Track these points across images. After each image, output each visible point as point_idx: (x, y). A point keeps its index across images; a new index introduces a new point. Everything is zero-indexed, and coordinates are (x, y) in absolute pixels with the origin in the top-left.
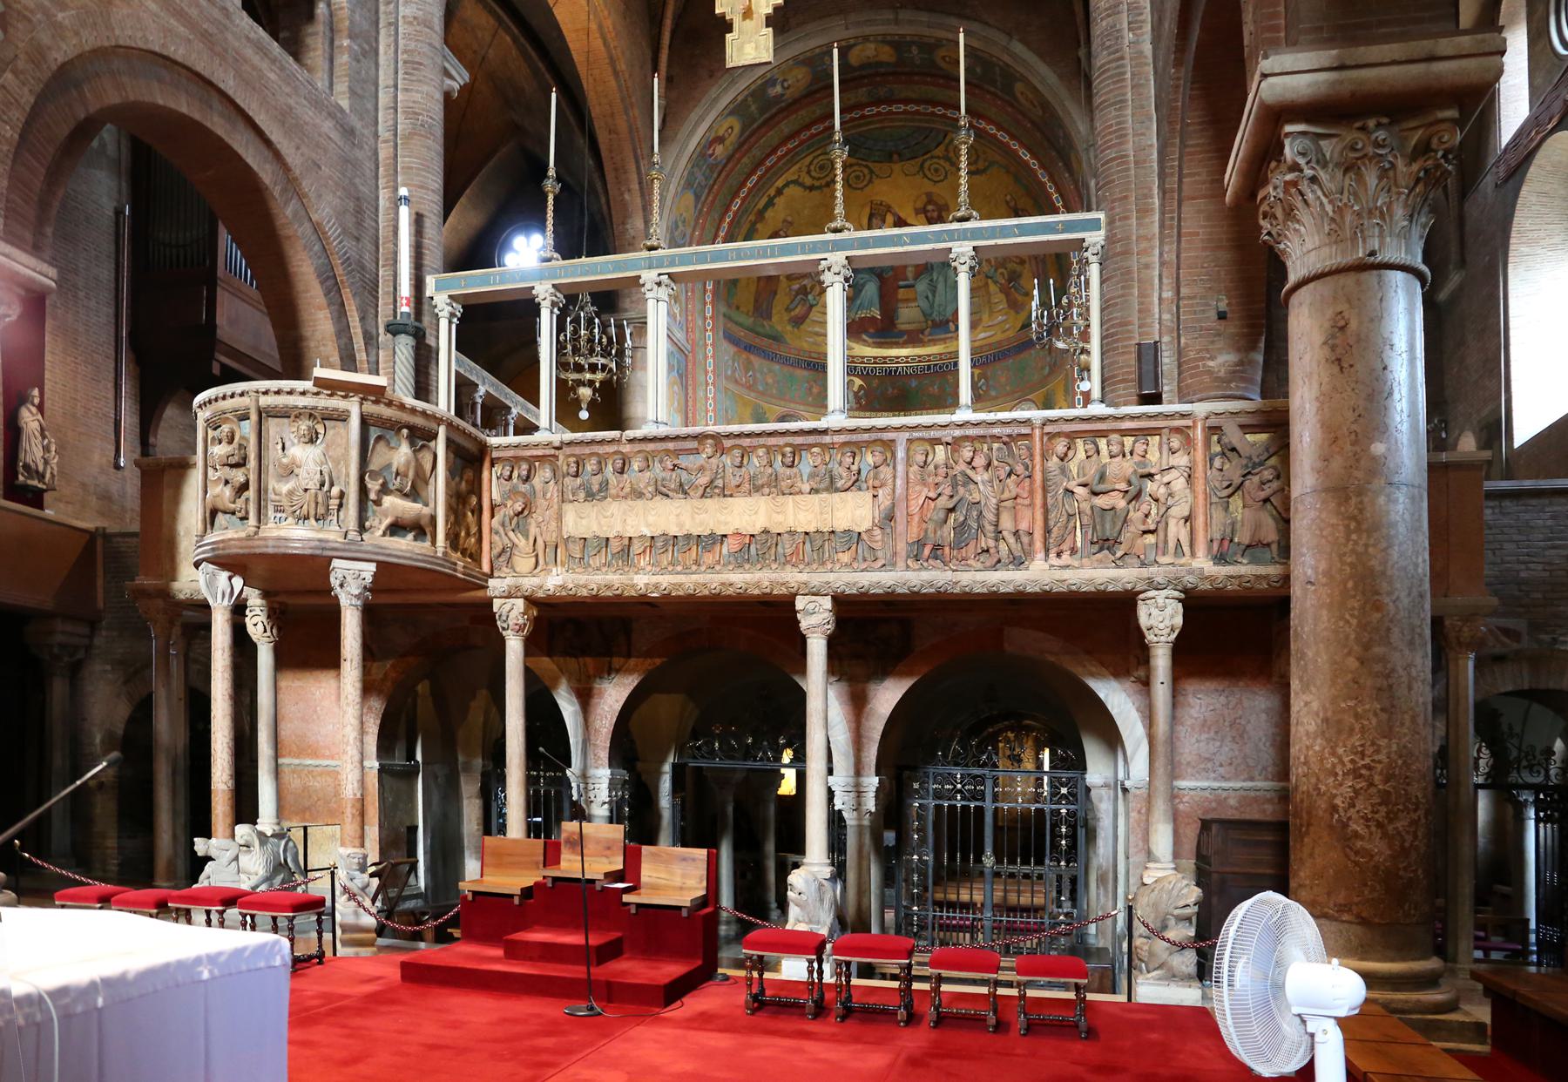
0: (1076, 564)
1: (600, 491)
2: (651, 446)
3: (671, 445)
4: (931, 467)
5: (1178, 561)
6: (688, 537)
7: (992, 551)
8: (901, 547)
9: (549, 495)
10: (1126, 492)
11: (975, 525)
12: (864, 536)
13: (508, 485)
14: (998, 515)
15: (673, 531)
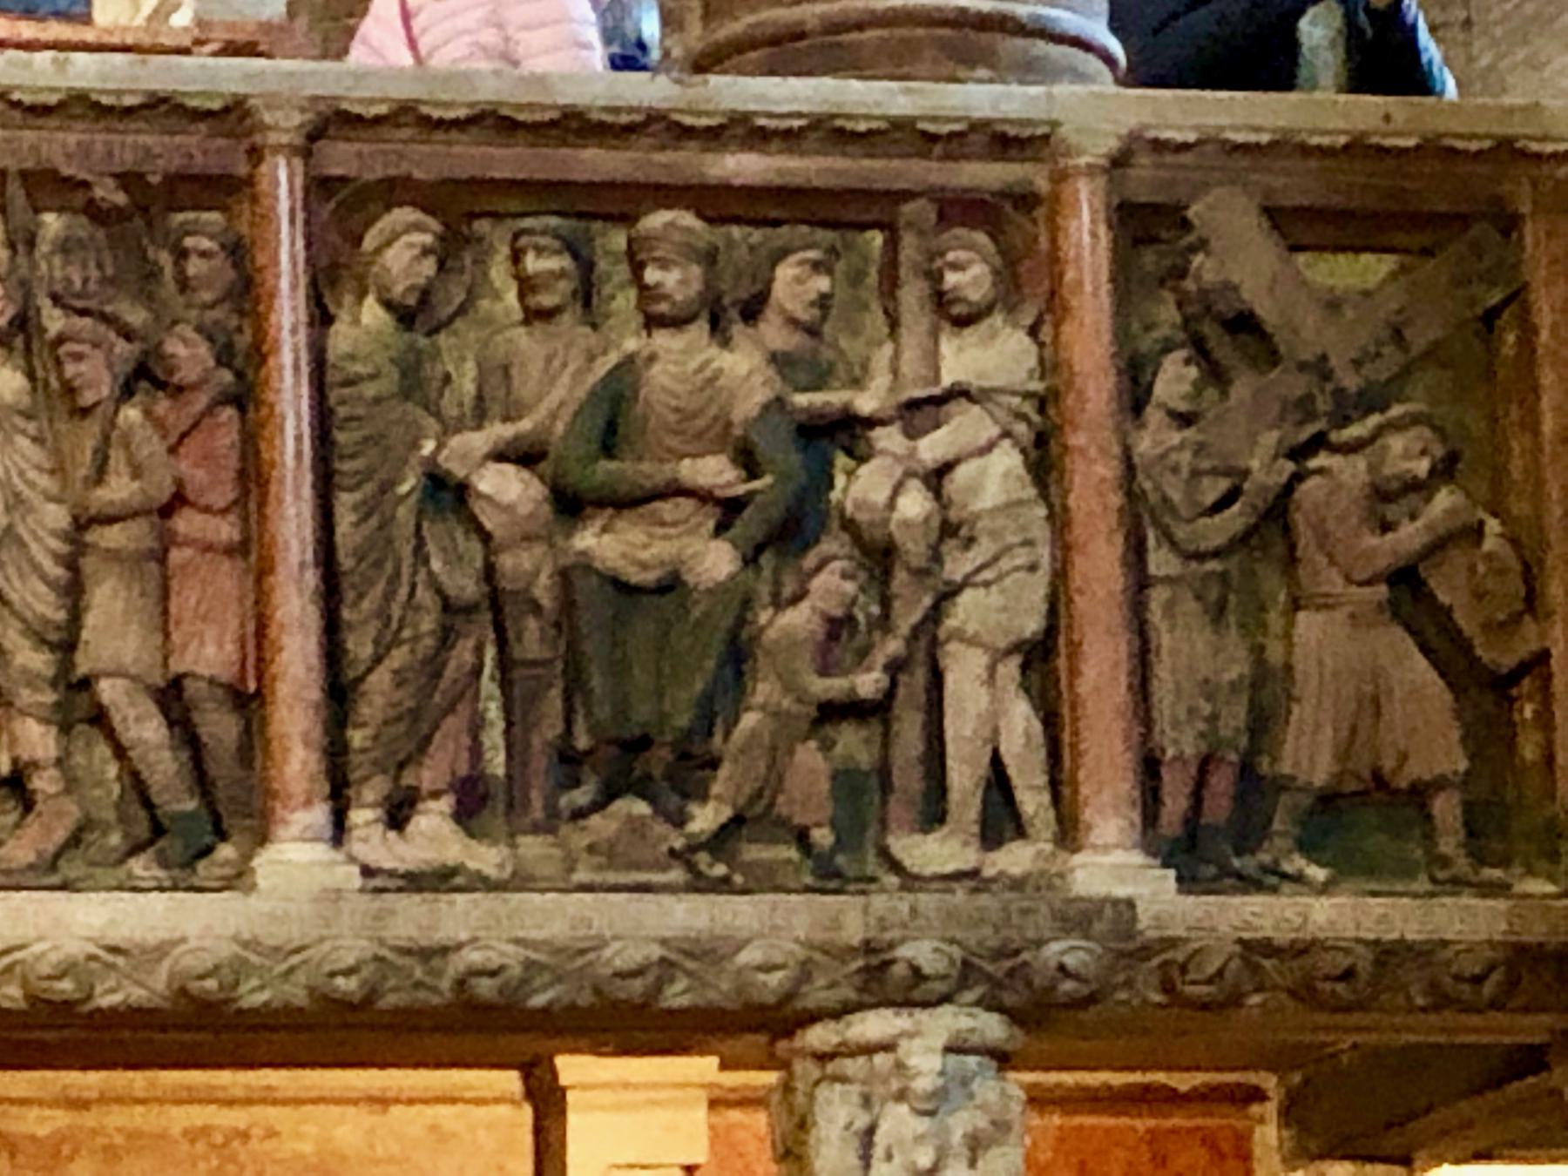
7: (44, 783)
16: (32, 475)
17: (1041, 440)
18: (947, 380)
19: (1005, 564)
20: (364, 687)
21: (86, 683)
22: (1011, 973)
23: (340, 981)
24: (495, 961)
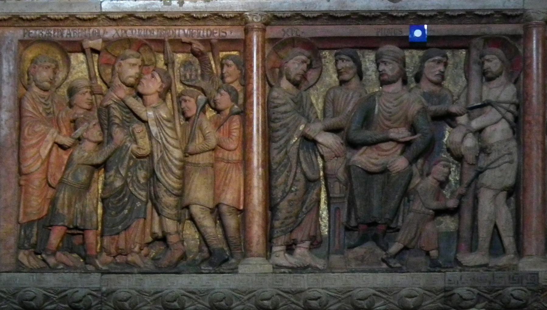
0: (320, 263)
4: (63, 91)
5: (494, 262)
7: (172, 239)
10: (407, 144)
11: (142, 195)
14: (184, 177)
16: (169, 139)
17: (516, 119)
18: (484, 99)
19: (500, 161)
20: (278, 207)
21: (188, 207)
22: (496, 297)
23: (265, 302)
24: (317, 295)
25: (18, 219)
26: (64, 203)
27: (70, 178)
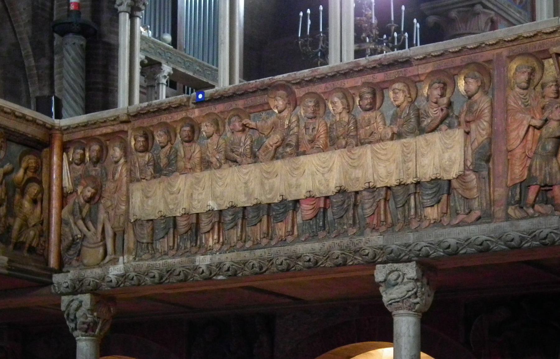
1: (169, 164)
2: (220, 107)
3: (240, 103)
6: (258, 207)
8: (500, 193)
9: (117, 176)
12: (455, 184)
13: (80, 169)
15: (242, 201)
25: (507, 184)
26: (536, 168)
27: (540, 149)
